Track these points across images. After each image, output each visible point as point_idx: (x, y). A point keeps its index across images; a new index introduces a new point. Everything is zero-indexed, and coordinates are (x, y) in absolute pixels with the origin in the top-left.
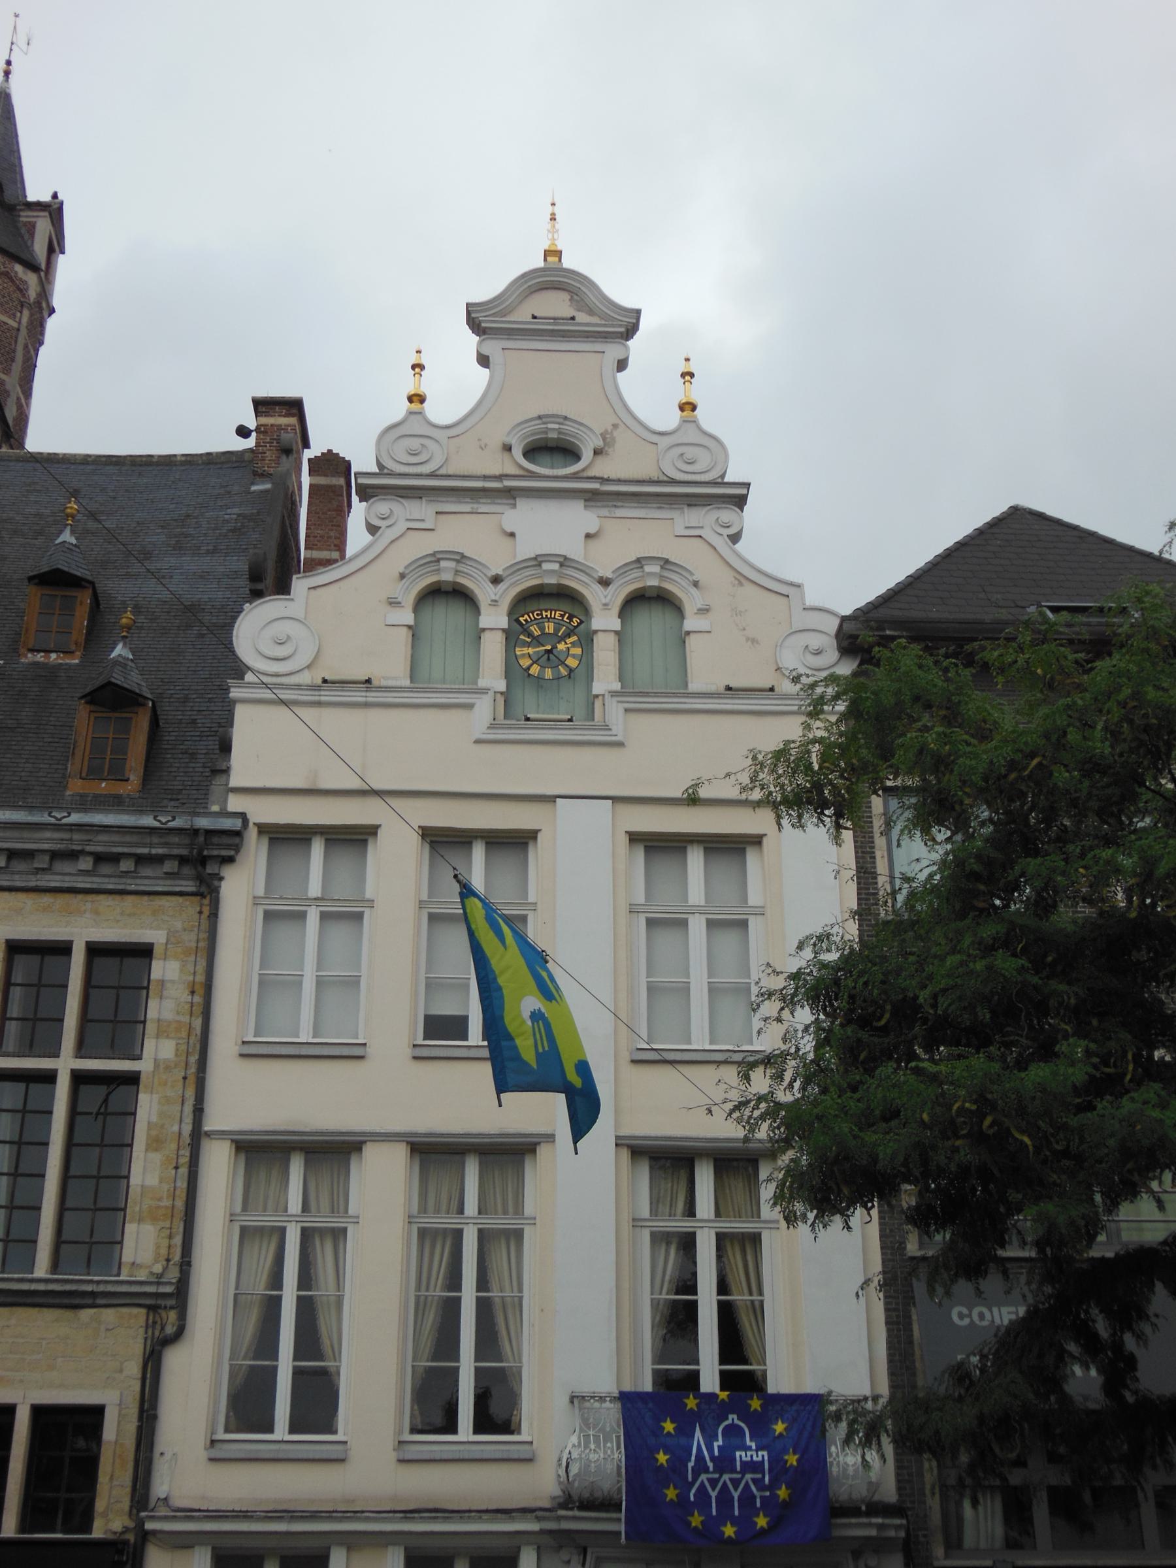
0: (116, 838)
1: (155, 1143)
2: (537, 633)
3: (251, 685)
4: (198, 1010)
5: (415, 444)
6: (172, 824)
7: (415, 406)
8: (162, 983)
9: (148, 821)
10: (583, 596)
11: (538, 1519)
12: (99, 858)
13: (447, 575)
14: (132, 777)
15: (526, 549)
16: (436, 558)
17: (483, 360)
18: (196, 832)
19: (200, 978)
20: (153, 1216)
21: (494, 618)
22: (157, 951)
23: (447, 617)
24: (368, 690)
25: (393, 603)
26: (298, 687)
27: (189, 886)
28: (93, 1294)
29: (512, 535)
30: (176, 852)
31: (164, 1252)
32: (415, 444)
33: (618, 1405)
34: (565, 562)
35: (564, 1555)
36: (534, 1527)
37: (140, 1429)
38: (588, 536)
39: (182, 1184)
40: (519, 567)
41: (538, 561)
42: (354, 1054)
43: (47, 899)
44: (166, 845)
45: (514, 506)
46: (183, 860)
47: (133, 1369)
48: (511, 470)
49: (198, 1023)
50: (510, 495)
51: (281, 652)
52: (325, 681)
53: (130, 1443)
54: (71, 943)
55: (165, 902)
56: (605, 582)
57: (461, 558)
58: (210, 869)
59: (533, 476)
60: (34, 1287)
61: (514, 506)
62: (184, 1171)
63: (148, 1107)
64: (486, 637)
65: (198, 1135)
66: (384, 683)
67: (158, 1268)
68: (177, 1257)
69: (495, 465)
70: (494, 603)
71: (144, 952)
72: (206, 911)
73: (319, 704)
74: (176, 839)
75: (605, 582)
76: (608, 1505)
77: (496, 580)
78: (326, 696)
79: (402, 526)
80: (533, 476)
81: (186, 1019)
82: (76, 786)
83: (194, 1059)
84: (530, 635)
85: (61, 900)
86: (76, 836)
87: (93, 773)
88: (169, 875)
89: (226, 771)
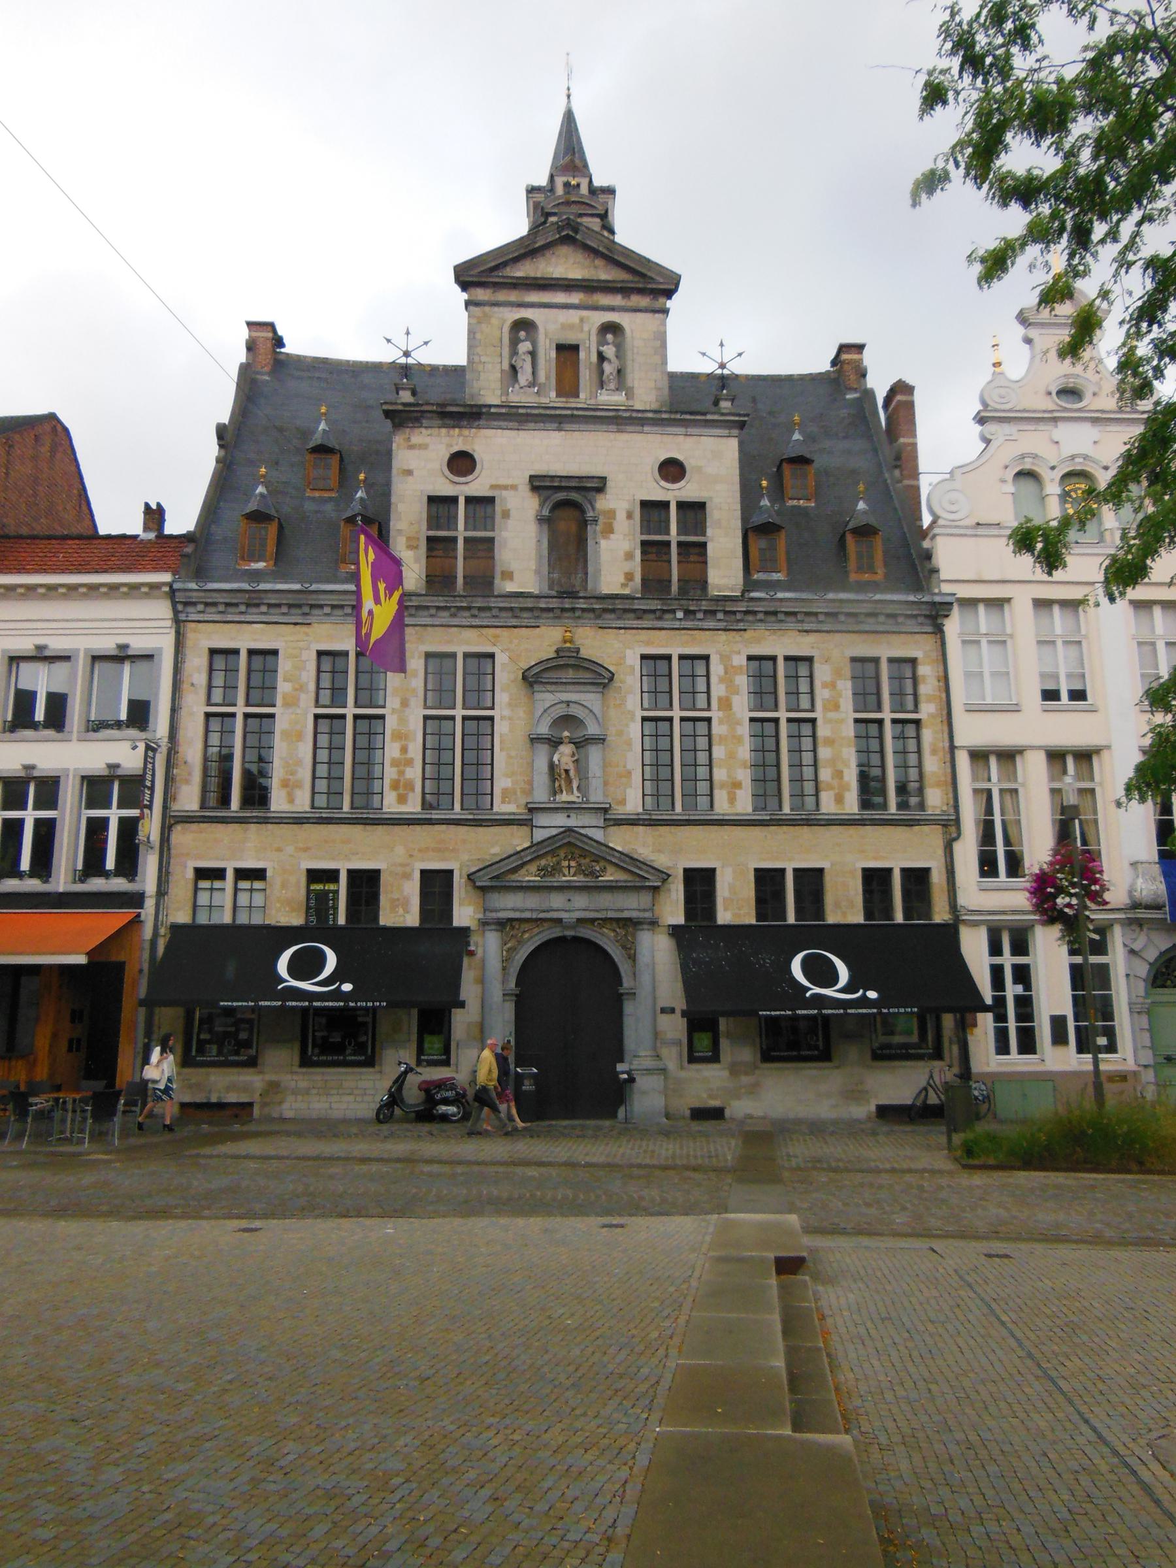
0: (896, 606)
1: (934, 752)
2: (1074, 496)
3: (944, 526)
4: (943, 688)
5: (1002, 391)
6: (923, 600)
7: (998, 370)
8: (923, 676)
9: (911, 598)
10: (1096, 478)
11: (1125, 913)
12: (888, 616)
13: (1027, 465)
14: (879, 571)
15: (1067, 450)
16: (1023, 457)
17: (1028, 341)
18: (934, 604)
19: (942, 674)
20: (938, 784)
21: (1053, 488)
22: (919, 661)
23: (1028, 485)
24: (1001, 528)
25: (1003, 481)
26: (967, 527)
27: (929, 629)
28: (919, 820)
29: (1057, 442)
30: (924, 613)
31: (945, 801)
32: (1002, 391)
33: (1158, 866)
34: (1086, 457)
35: (1133, 927)
36: (1123, 916)
37: (948, 878)
38: (1095, 442)
39: (949, 770)
40: (1063, 461)
41: (1073, 457)
42: (1015, 709)
43: (864, 636)
44: (919, 609)
45: (1056, 427)
46: (926, 616)
47: (940, 852)
48: (1051, 407)
49: (944, 695)
50: (1055, 420)
51: (953, 508)
52: (978, 524)
53: (944, 883)
54: (879, 658)
55: (917, 636)
56: (1106, 468)
57: (1035, 456)
58: (939, 621)
59: (1065, 410)
60: (890, 817)
61: (1056, 427)
62: (948, 764)
63: (927, 735)
64: (1047, 499)
65: (952, 748)
66: (1006, 525)
67: (945, 808)
68: (951, 802)
69: (1048, 404)
70: (1052, 480)
71: (913, 662)
72: (939, 641)
73: (976, 536)
74: (924, 607)
75: (1106, 468)
76: (1158, 907)
77: (1053, 468)
78: (980, 531)
79: (1001, 439)
80: (1065, 410)
81: (938, 693)
82: (853, 577)
83: (945, 712)
84: (1070, 497)
85: (872, 636)
86: (879, 606)
87: (860, 569)
88: (921, 624)
89: (937, 571)
